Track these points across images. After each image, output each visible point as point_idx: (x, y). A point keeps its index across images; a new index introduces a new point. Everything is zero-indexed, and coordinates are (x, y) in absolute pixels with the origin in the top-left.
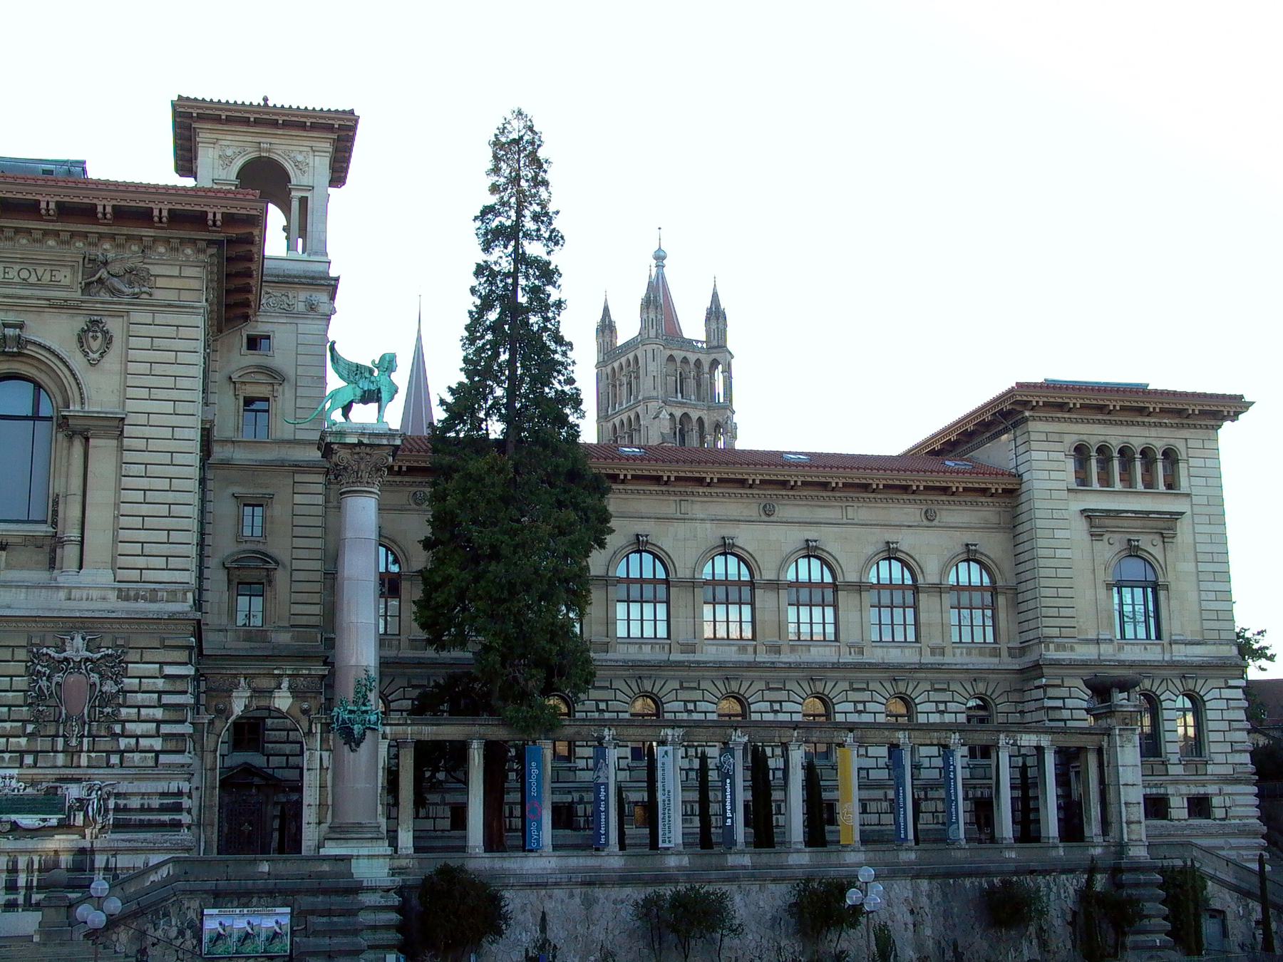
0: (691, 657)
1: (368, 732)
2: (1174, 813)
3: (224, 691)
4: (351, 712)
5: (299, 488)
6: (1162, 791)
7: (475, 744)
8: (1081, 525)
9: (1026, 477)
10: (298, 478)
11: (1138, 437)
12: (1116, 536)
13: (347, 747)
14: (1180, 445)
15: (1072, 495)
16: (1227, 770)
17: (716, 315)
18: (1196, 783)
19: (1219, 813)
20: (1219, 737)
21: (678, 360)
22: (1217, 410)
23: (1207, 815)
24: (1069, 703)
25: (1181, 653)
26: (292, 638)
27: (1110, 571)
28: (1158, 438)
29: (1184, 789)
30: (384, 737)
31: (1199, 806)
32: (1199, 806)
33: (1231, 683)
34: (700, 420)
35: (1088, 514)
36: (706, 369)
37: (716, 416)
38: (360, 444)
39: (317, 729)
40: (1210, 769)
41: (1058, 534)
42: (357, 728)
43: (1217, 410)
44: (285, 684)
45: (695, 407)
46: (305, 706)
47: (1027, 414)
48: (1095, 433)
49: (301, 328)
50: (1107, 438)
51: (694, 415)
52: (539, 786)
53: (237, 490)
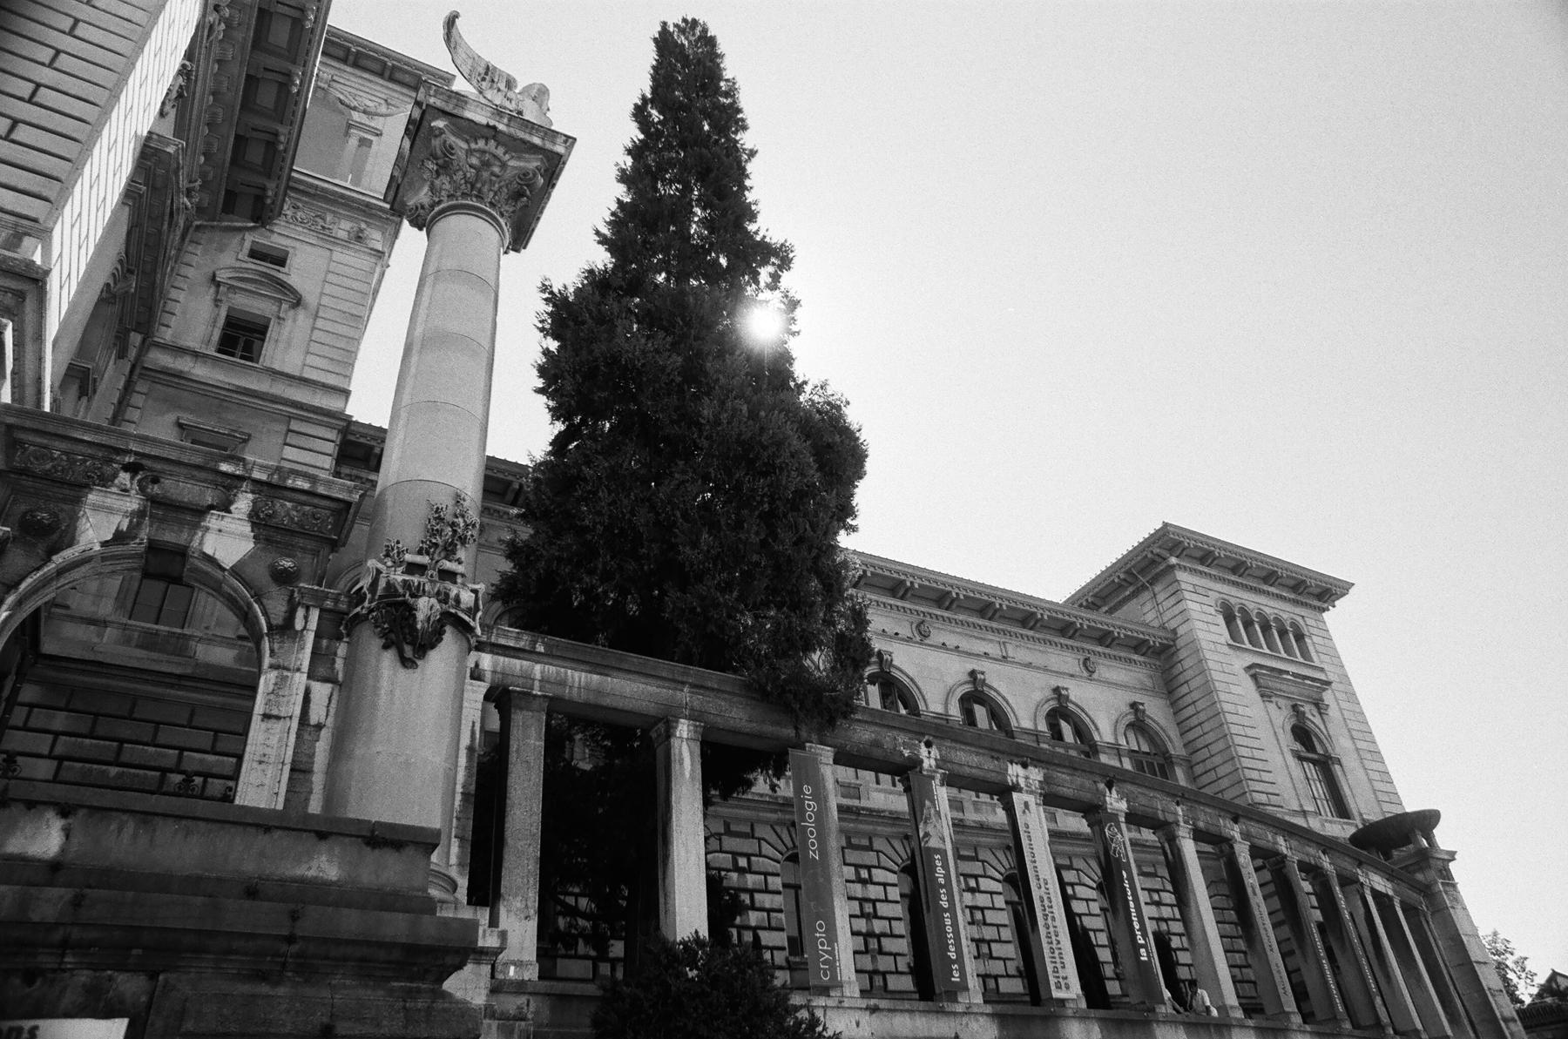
0: (855, 803)
1: (449, 635)
3: (72, 485)
4: (413, 568)
5: (292, 439)
7: (684, 729)
8: (1247, 687)
9: (1181, 631)
10: (295, 425)
13: (388, 659)
15: (1231, 652)
22: (1323, 592)
26: (238, 659)
30: (477, 675)
35: (1254, 671)
38: (491, 132)
39: (308, 622)
41: (1233, 689)
42: (425, 607)
43: (1323, 592)
44: (243, 503)
46: (287, 563)
47: (1173, 560)
49: (337, 256)
52: (822, 839)
53: (187, 418)
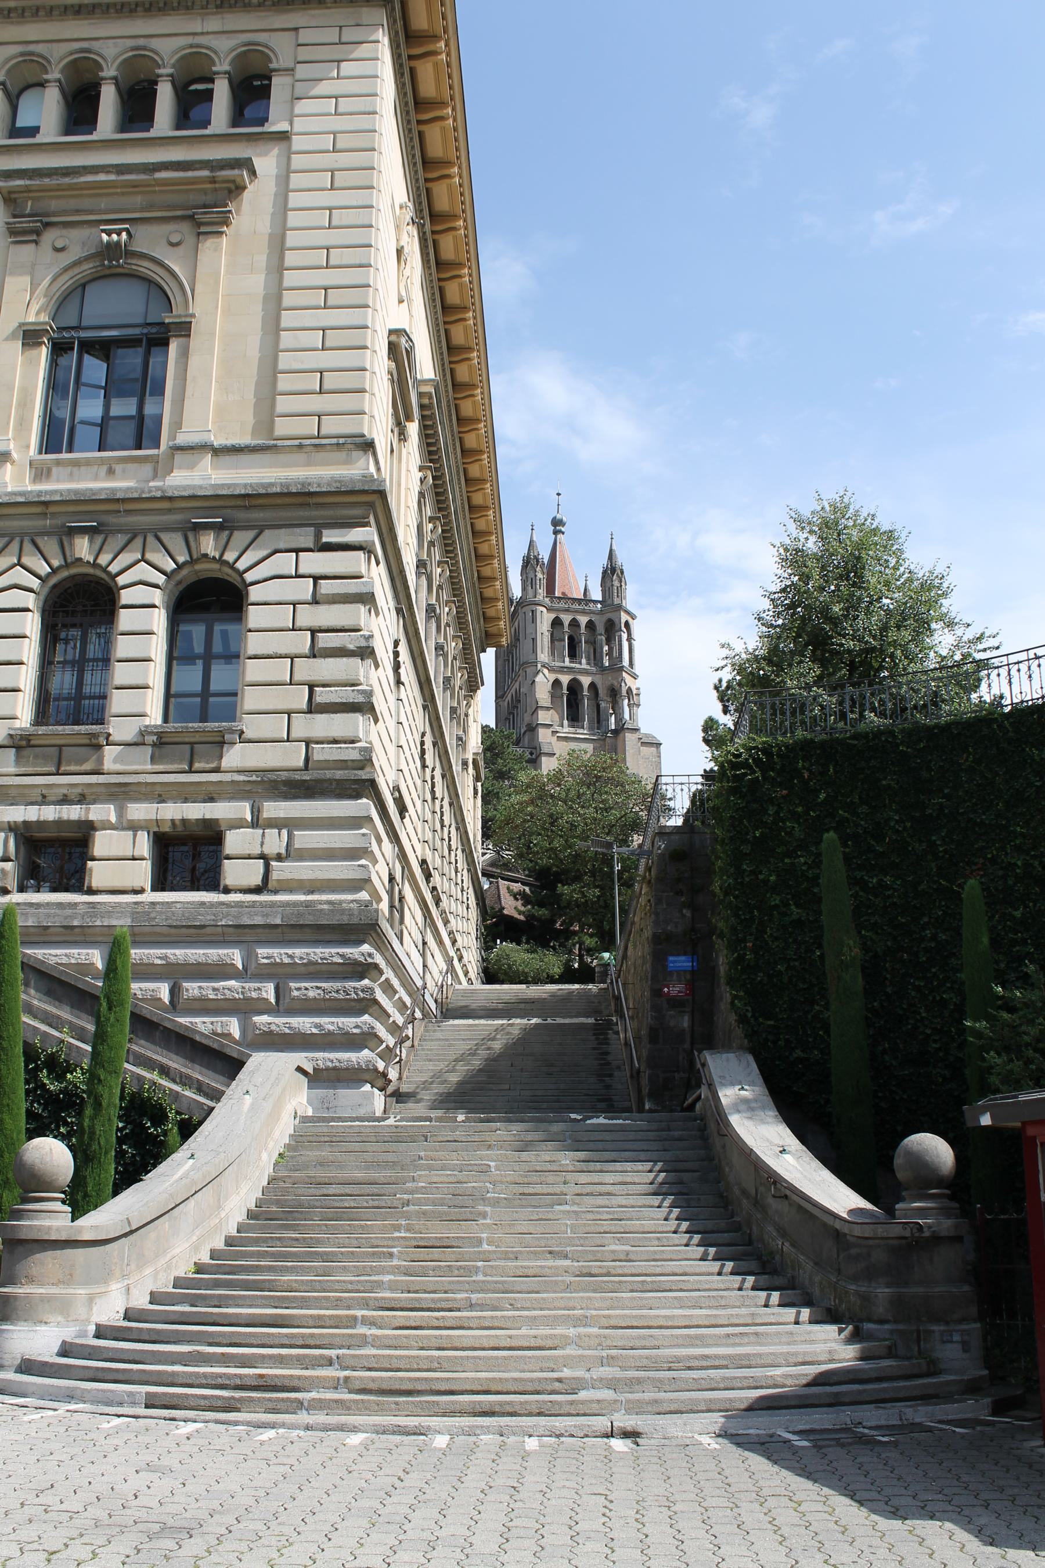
2: (99, 873)
6: (73, 813)
12: (75, 234)
16: (294, 757)
17: (612, 573)
18: (186, 794)
20: (281, 670)
21: (566, 623)
23: (208, 878)
33: (330, 536)
34: (593, 686)
36: (600, 628)
37: (610, 679)
40: (235, 757)
45: (586, 672)
50: (95, 45)
51: (586, 681)
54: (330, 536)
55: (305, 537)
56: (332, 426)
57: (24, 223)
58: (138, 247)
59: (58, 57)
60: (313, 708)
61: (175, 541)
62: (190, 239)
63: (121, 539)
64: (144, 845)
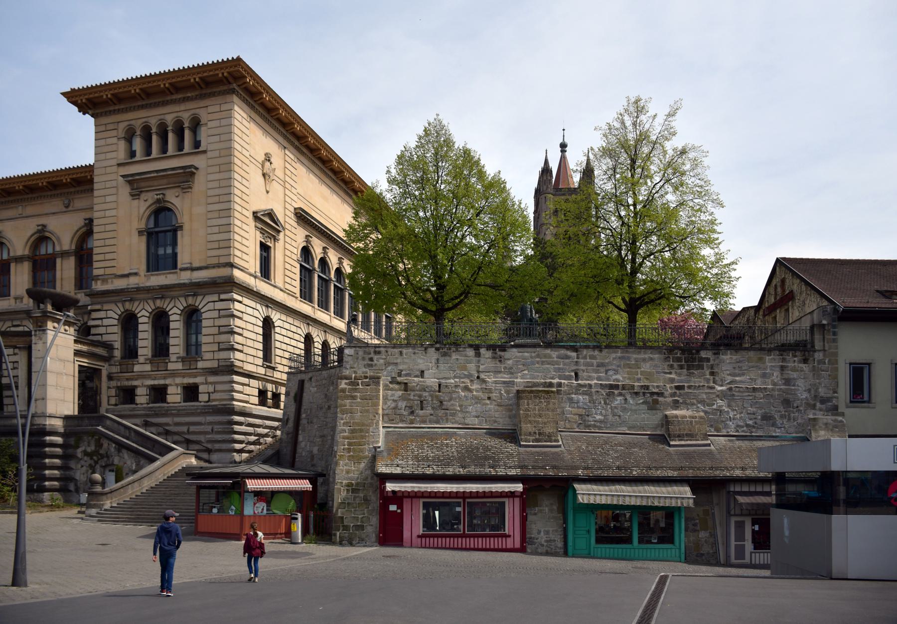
2: (170, 398)
6: (162, 382)
8: (125, 190)
11: (169, 114)
12: (150, 194)
14: (204, 116)
16: (215, 364)
19: (203, 397)
24: (106, 322)
25: (185, 277)
27: (144, 221)
28: (183, 112)
29: (178, 380)
31: (191, 392)
32: (191, 392)
33: (223, 296)
40: (201, 365)
48: (138, 118)
54: (223, 296)
55: (215, 297)
56: (223, 260)
57: (135, 192)
58: (167, 199)
59: (138, 125)
60: (220, 350)
61: (182, 300)
62: (181, 194)
63: (168, 300)
64: (179, 390)
